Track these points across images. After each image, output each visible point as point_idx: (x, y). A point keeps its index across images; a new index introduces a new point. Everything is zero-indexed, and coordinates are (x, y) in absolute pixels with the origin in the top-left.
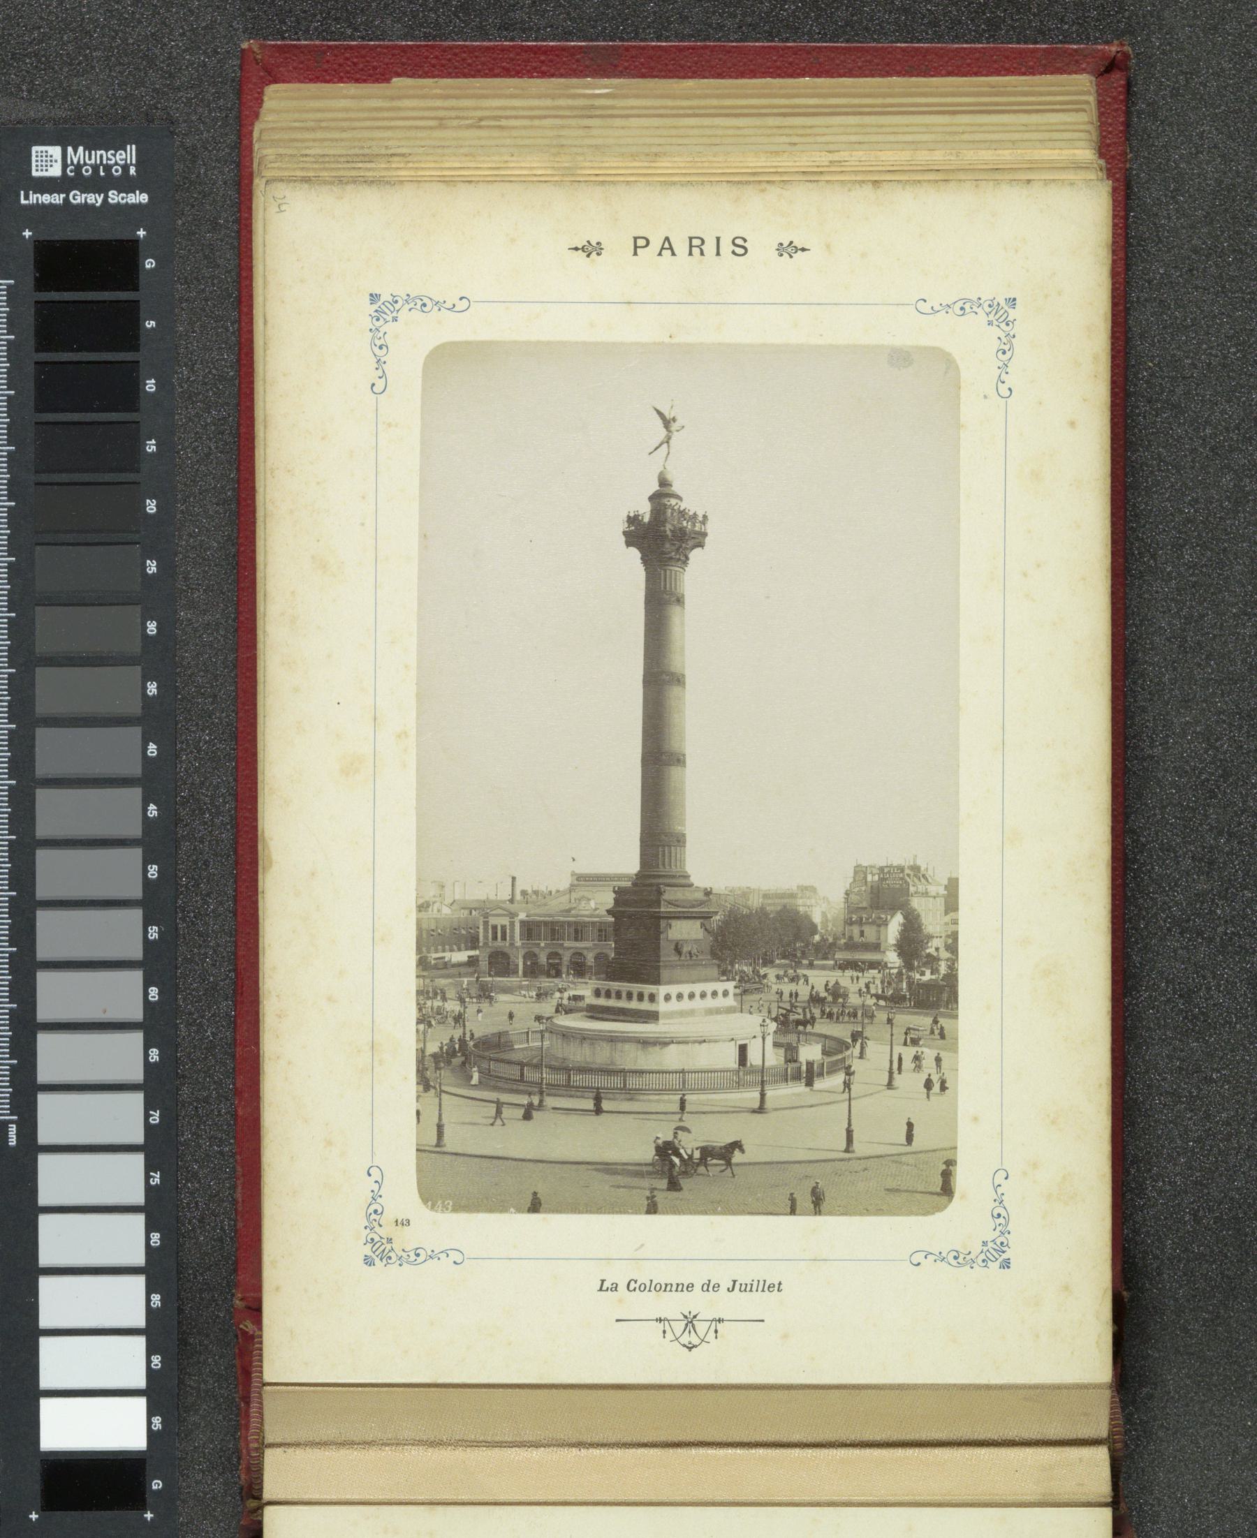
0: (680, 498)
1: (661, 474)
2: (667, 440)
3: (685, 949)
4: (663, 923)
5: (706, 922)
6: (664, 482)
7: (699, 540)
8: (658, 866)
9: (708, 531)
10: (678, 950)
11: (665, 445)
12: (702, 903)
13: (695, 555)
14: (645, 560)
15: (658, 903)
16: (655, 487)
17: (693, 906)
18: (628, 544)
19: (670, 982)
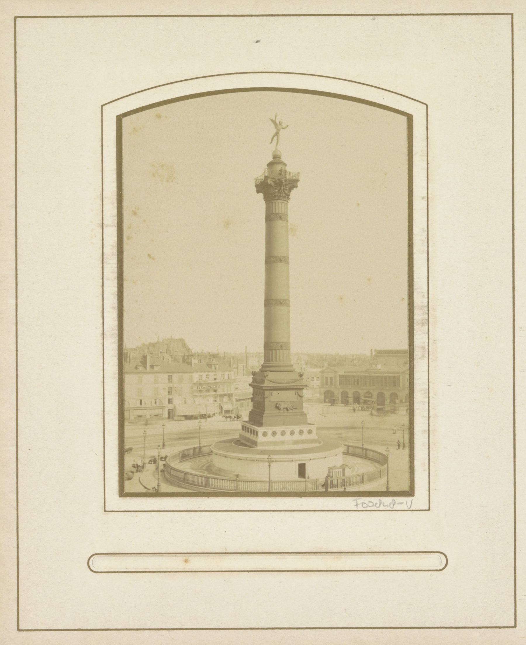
0: (286, 165)
1: (275, 151)
2: (277, 134)
3: (283, 406)
4: (267, 393)
5: (299, 392)
6: (276, 157)
7: (293, 184)
8: (272, 361)
9: (300, 179)
10: (277, 408)
11: (276, 137)
12: (296, 381)
13: (294, 193)
14: (265, 198)
15: (263, 382)
16: (270, 159)
17: (289, 383)
18: (258, 192)
19: (271, 425)
